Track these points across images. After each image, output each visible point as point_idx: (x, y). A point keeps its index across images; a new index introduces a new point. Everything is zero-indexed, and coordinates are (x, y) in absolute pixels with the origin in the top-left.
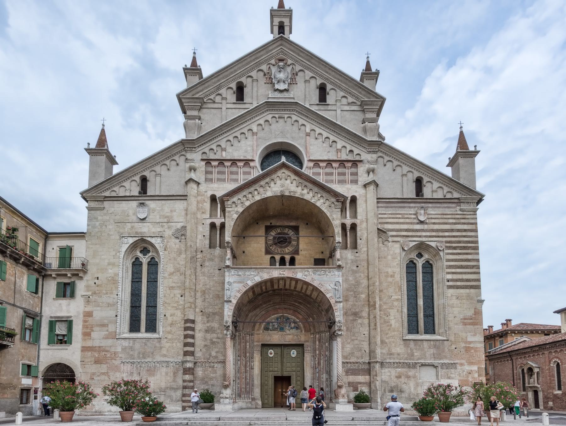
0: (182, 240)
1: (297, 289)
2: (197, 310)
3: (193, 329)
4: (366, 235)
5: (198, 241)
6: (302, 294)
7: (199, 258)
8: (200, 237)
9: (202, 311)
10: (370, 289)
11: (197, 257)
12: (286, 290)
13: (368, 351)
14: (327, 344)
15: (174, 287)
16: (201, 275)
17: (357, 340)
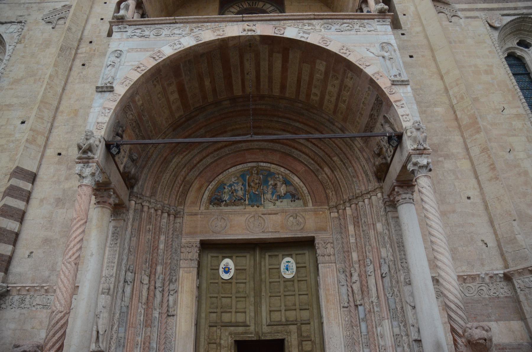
0: (57, 26)
1: (287, 95)
2: (51, 152)
3: (27, 197)
4: (412, 9)
5: (88, 27)
6: (300, 105)
7: (82, 53)
8: (94, 20)
9: (60, 154)
10: (451, 93)
11: (79, 51)
12: (262, 97)
13: (492, 243)
14: (379, 226)
15: (13, 106)
16: (77, 81)
17: (454, 212)
